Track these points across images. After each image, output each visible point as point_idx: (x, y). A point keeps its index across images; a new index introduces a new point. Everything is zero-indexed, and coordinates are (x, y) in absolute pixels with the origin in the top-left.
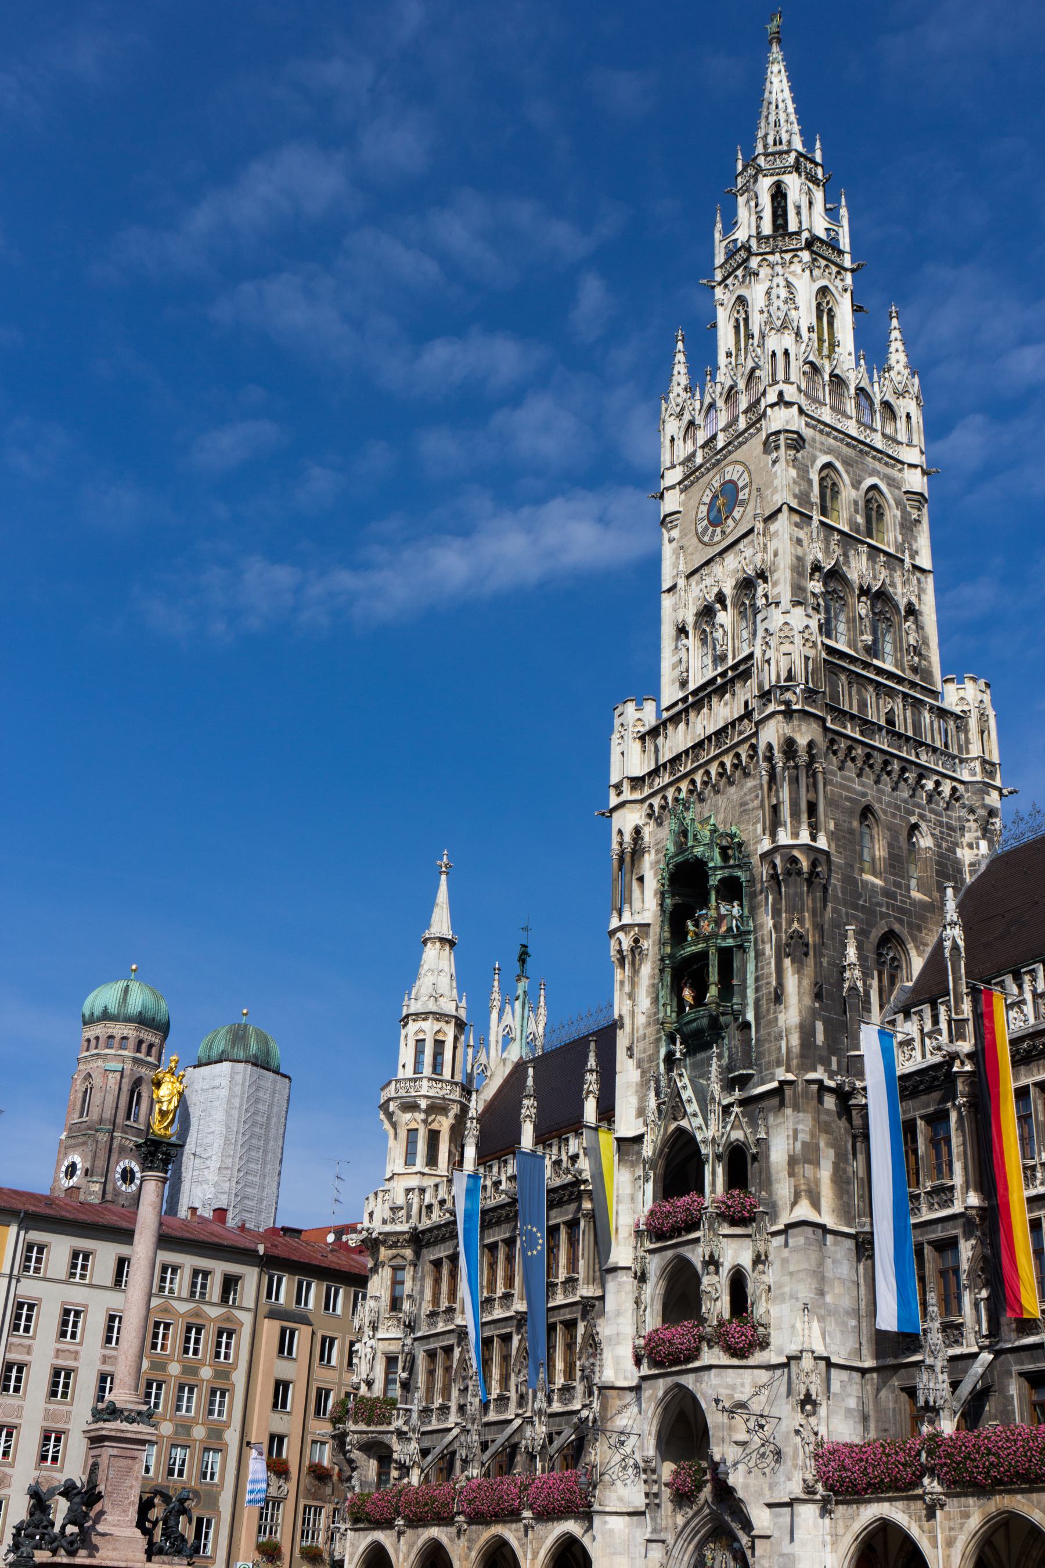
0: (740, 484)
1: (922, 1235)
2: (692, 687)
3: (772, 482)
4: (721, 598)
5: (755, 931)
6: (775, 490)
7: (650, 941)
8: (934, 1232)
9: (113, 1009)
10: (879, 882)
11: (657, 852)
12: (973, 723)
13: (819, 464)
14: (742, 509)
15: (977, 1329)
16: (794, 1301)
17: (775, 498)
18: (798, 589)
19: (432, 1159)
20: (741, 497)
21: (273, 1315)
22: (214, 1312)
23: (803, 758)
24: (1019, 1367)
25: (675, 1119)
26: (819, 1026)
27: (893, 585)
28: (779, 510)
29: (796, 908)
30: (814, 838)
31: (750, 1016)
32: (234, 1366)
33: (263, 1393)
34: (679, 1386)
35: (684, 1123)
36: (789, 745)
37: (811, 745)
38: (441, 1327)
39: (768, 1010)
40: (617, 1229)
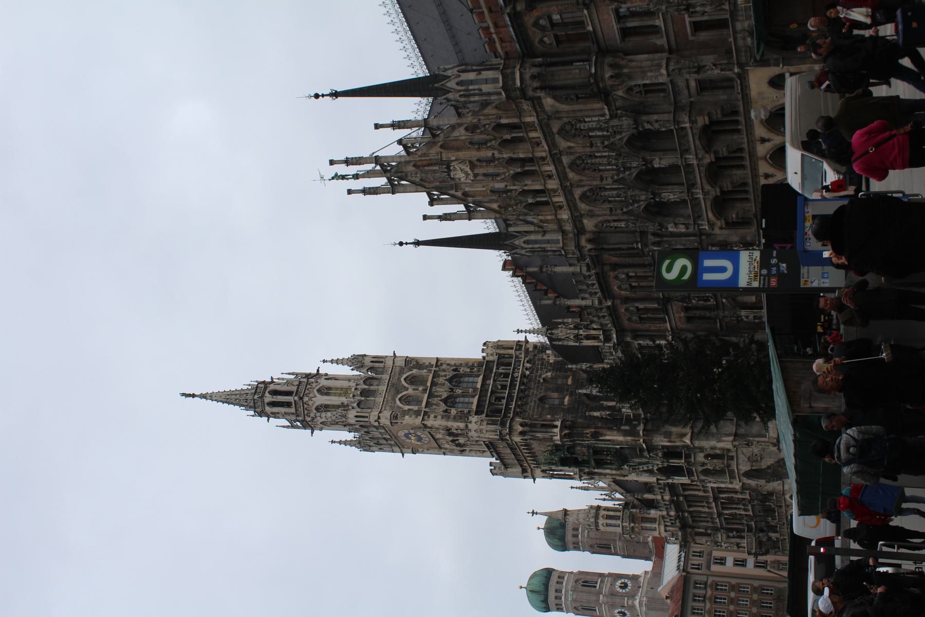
4: (453, 441)
9: (542, 598)
10: (567, 399)
12: (502, 352)
13: (400, 405)
18: (455, 419)
19: (653, 520)
21: (708, 568)
22: (709, 592)
23: (526, 429)
26: (623, 428)
27: (445, 376)
29: (582, 435)
30: (556, 427)
32: (729, 583)
33: (739, 570)
36: (522, 433)
37: (521, 425)
38: (717, 520)
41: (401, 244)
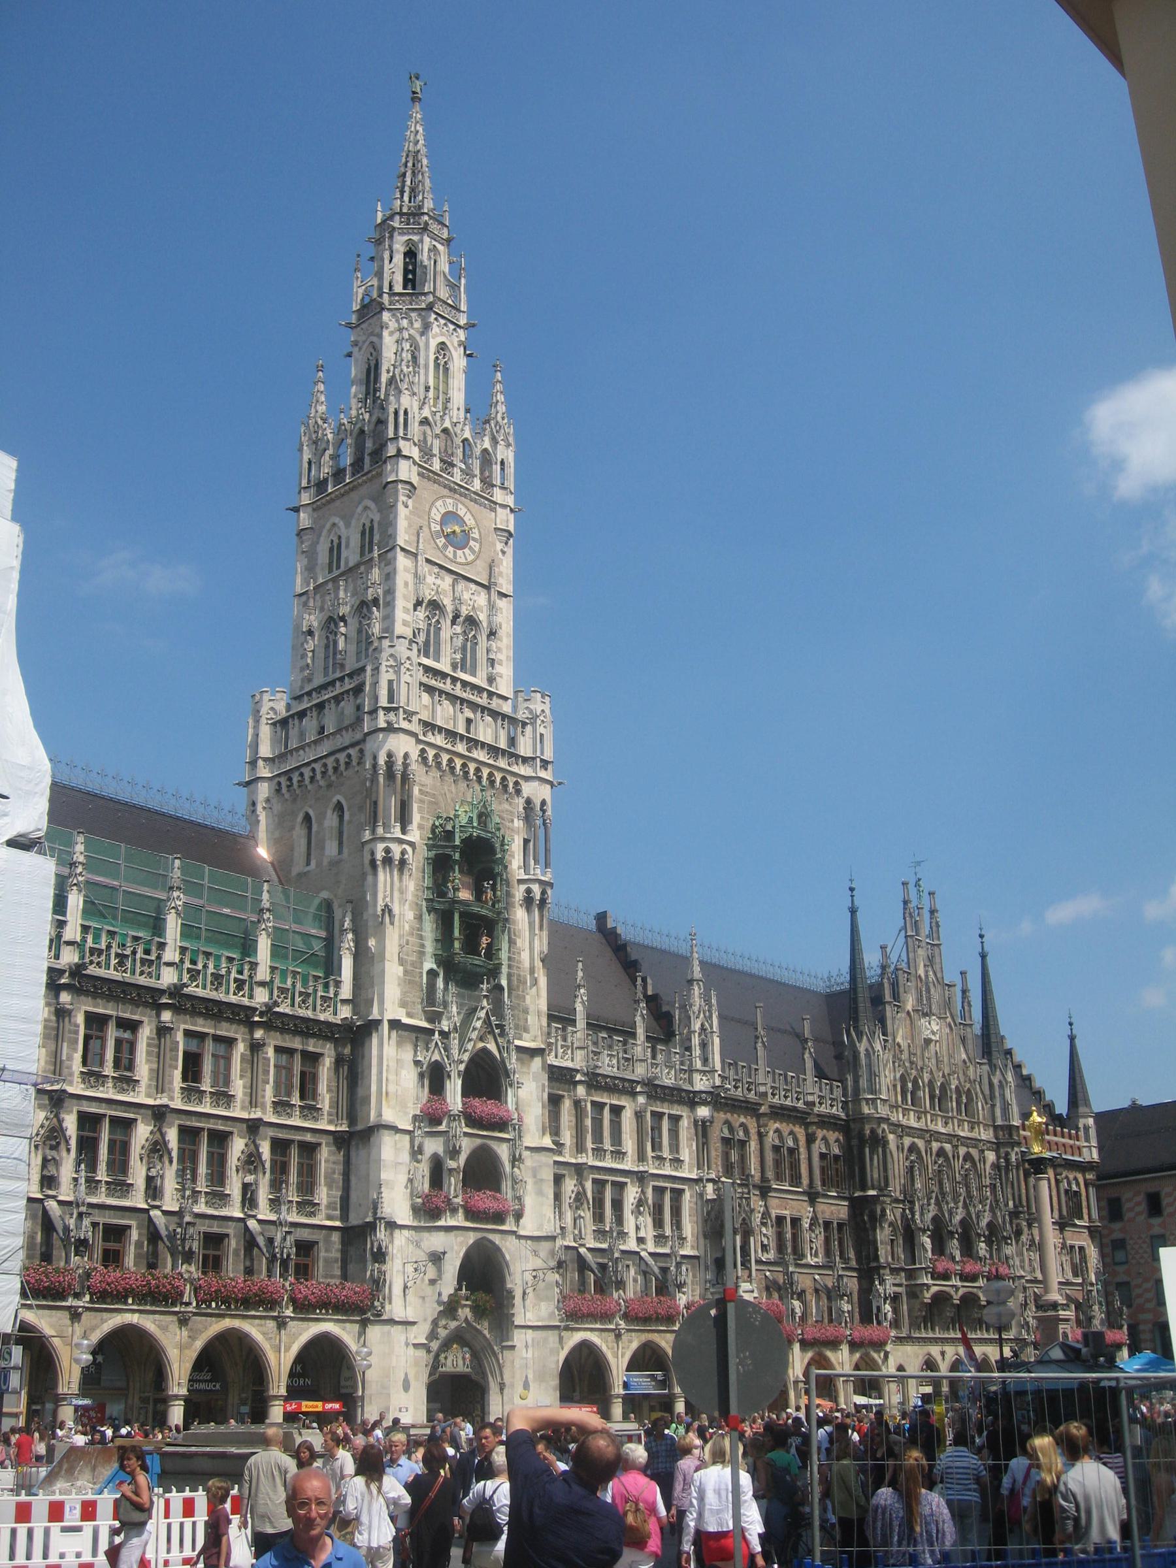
15: (576, 1232)
20: (472, 543)
28: (506, 596)
31: (504, 983)
34: (484, 1238)
35: (488, 1046)
40: (387, 1093)
41: (852, 889)
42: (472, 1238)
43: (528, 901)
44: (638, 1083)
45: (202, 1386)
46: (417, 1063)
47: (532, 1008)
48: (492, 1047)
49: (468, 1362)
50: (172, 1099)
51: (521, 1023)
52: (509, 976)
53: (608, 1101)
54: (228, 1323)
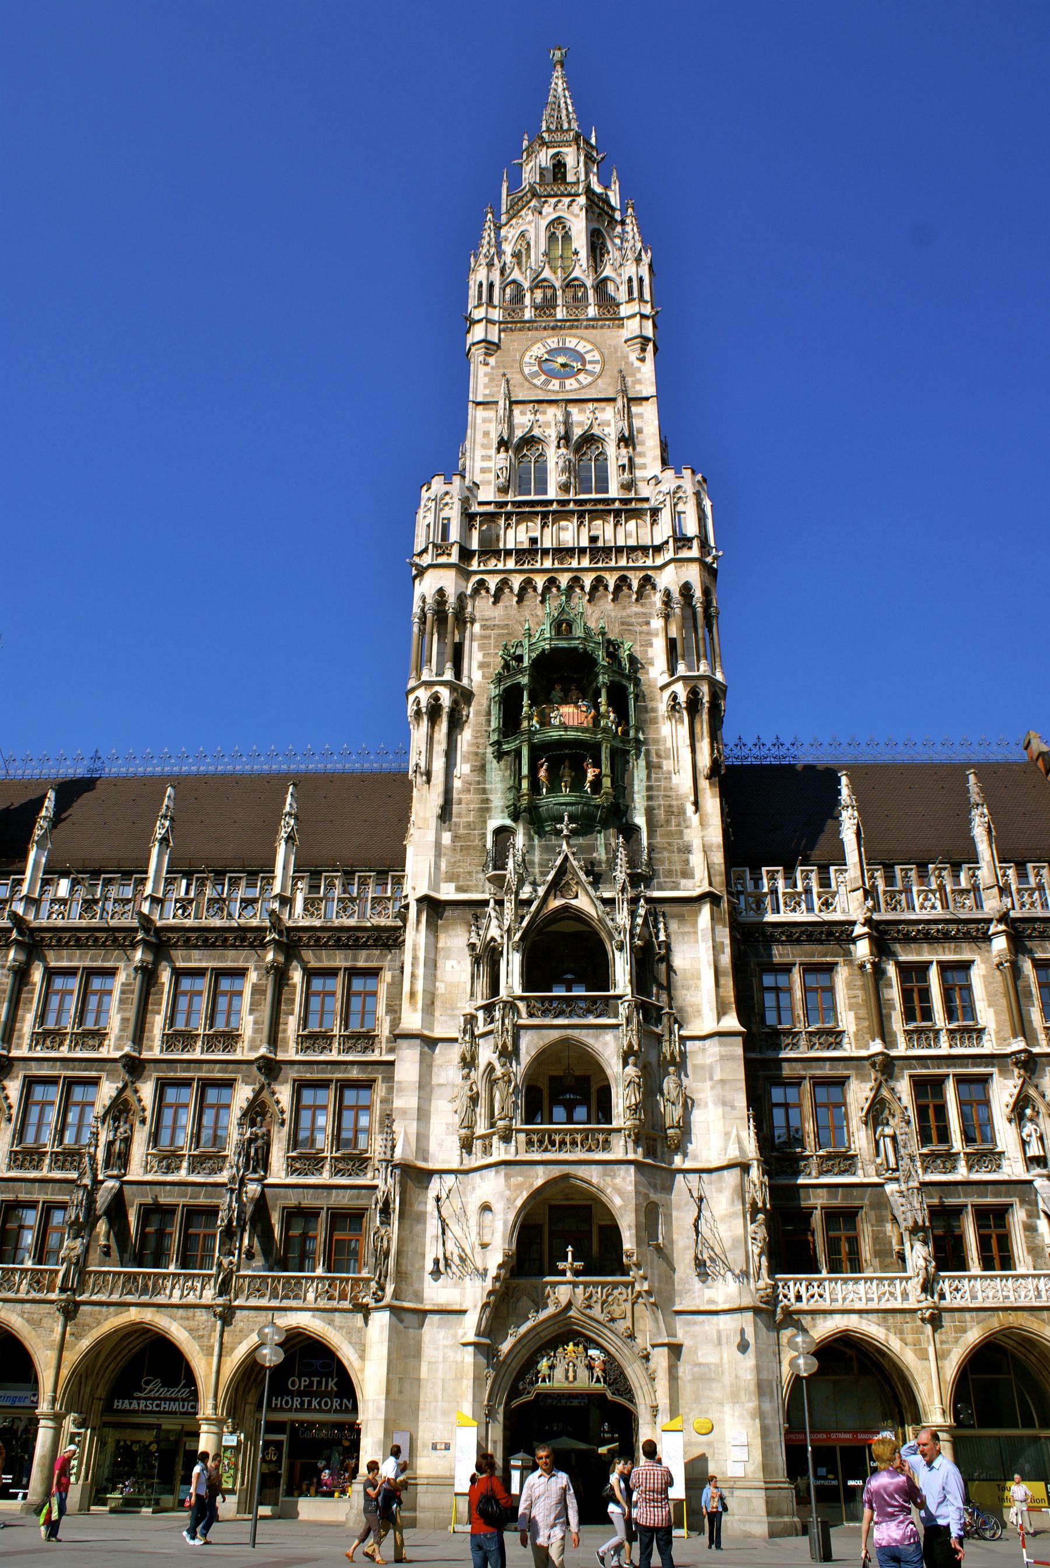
0: (588, 357)
1: (804, 1069)
2: (510, 497)
3: (634, 375)
5: (645, 742)
6: (639, 382)
7: (471, 709)
8: (821, 1069)
11: (484, 627)
14: (590, 379)
16: (728, 1109)
17: (638, 387)
20: (588, 367)
24: (929, 1201)
25: (563, 896)
28: (647, 399)
31: (640, 820)
34: (566, 1177)
35: (573, 902)
39: (668, 822)
40: (412, 994)
42: (540, 1177)
43: (674, 707)
44: (989, 921)
45: (175, 1406)
46: (472, 946)
47: (697, 845)
48: (583, 903)
49: (598, 1372)
50: (151, 1049)
51: (677, 867)
52: (649, 812)
53: (935, 958)
54: (133, 1315)
